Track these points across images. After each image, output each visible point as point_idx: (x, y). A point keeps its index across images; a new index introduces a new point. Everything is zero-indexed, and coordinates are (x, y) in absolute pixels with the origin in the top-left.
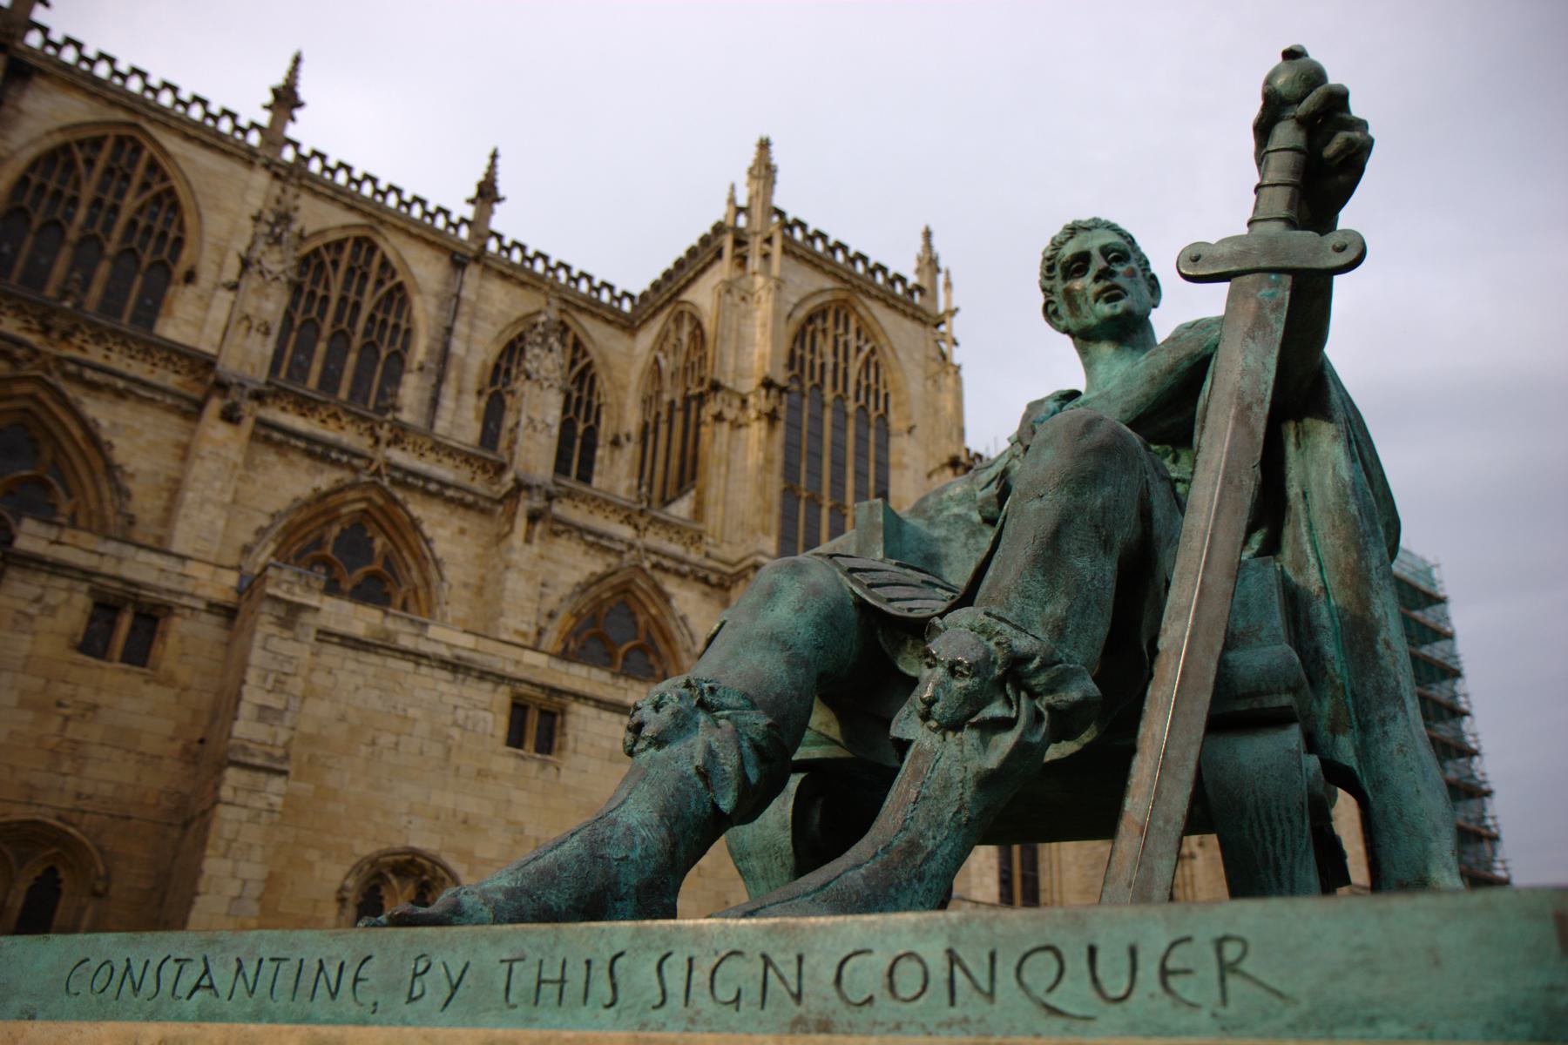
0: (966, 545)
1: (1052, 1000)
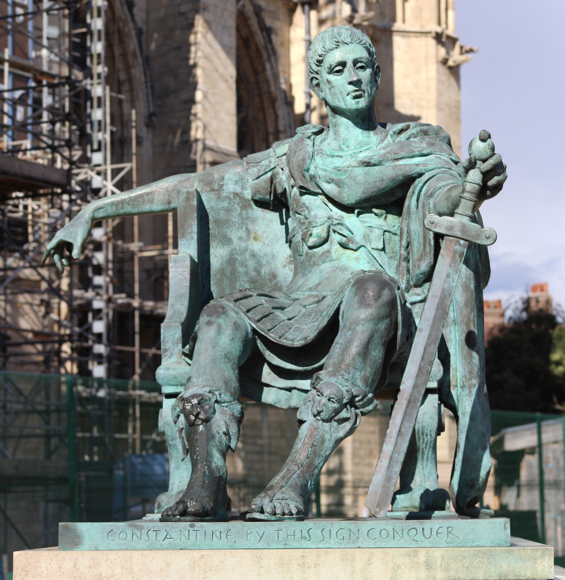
0: (240, 214)
1: (415, 538)
